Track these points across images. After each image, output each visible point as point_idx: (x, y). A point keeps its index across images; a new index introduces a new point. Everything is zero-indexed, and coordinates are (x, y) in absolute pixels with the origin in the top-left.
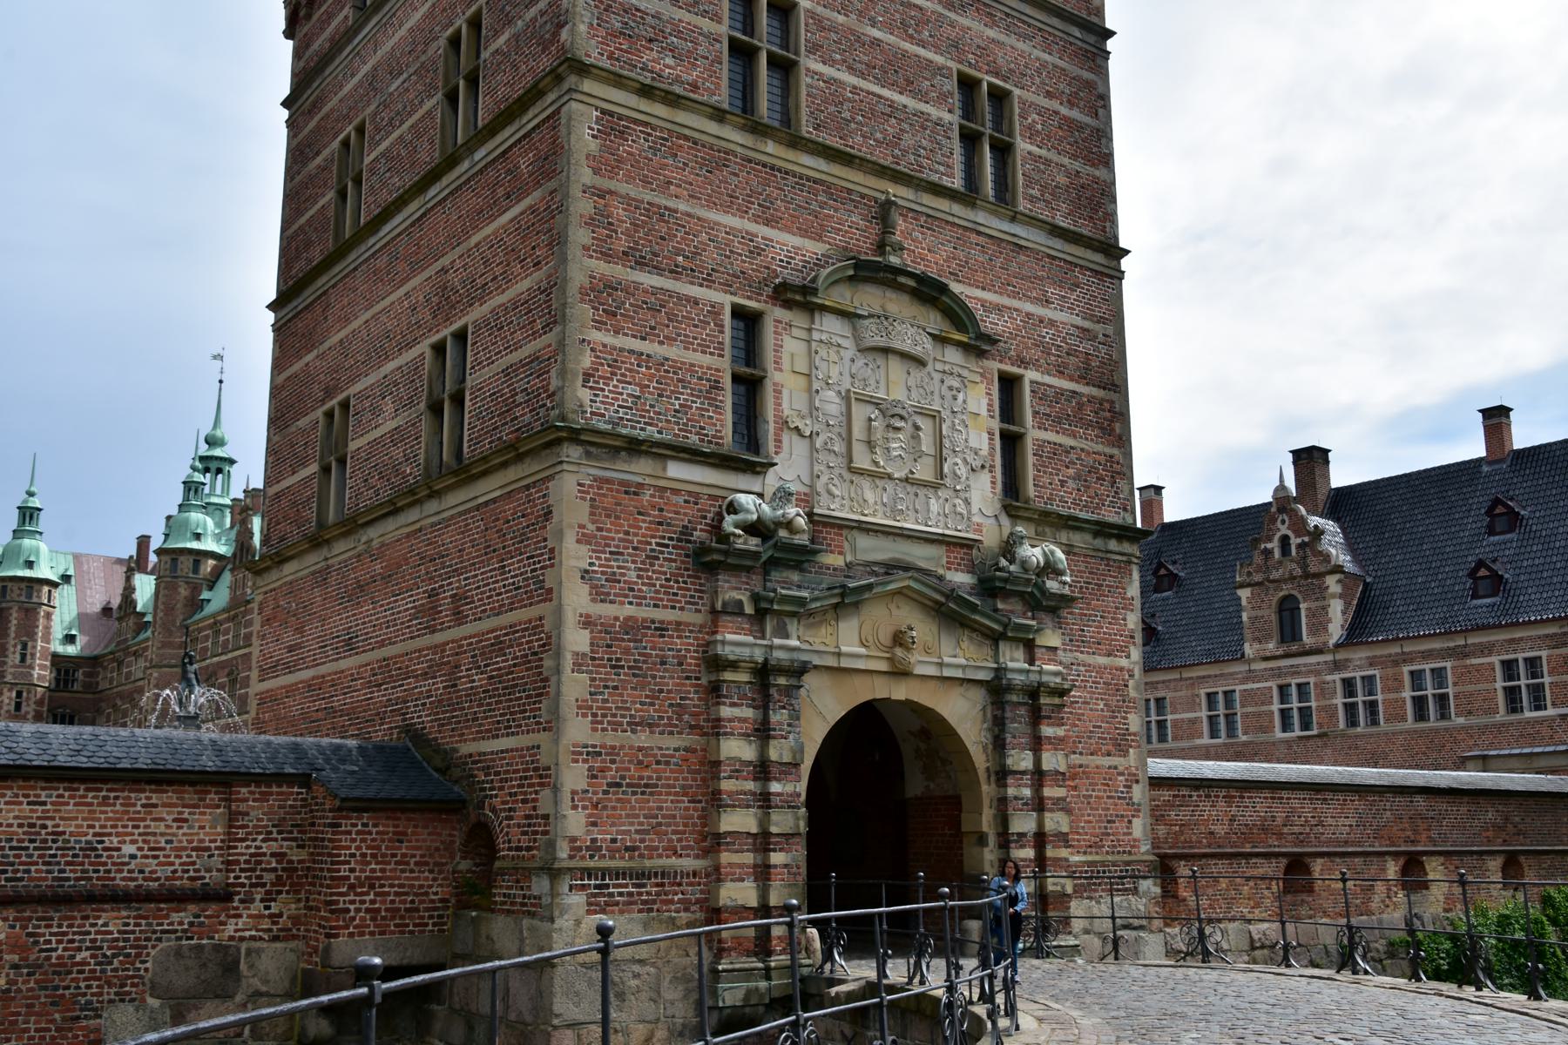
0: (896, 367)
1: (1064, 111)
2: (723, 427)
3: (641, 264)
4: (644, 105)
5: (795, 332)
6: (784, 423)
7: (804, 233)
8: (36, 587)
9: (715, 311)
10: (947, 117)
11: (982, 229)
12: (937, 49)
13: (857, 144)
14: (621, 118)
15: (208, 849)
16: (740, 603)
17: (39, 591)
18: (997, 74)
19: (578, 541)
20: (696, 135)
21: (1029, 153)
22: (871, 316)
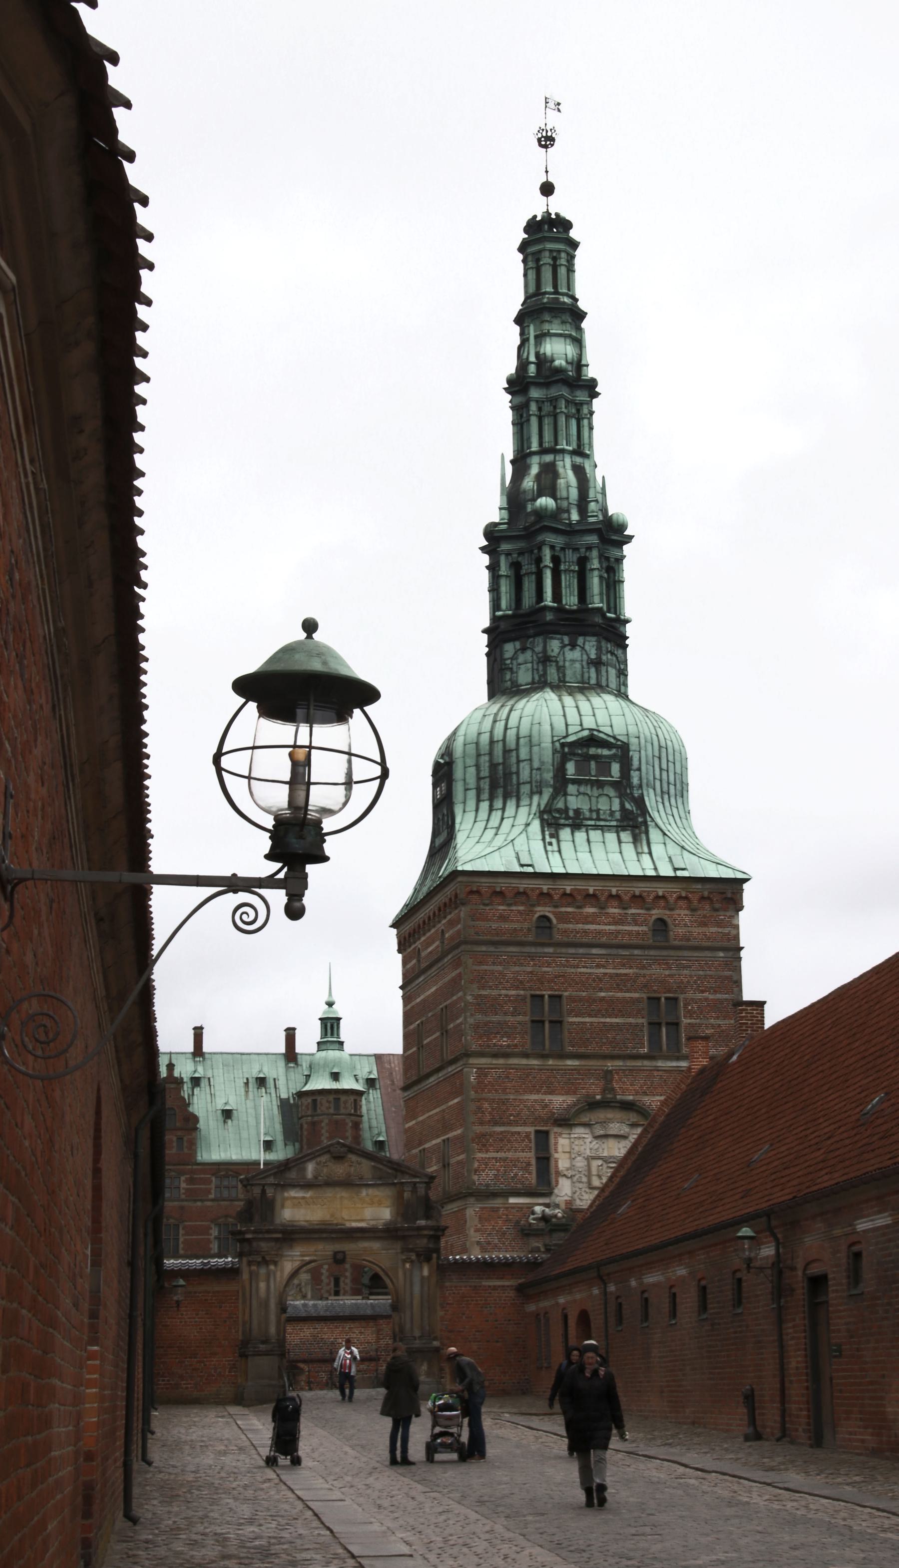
0: (612, 1142)
1: (711, 997)
2: (532, 1178)
3: (496, 1124)
4: (495, 1061)
5: (564, 1136)
6: (558, 1174)
7: (567, 1093)
8: (343, 1098)
9: (528, 1135)
10: (640, 1021)
11: (660, 1068)
12: (635, 991)
13: (591, 1049)
14: (485, 1069)
15: (370, 1343)
16: (538, 1248)
17: (345, 1102)
18: (669, 991)
19: (475, 1231)
20: (517, 1066)
21: (689, 1024)
22: (597, 1123)
